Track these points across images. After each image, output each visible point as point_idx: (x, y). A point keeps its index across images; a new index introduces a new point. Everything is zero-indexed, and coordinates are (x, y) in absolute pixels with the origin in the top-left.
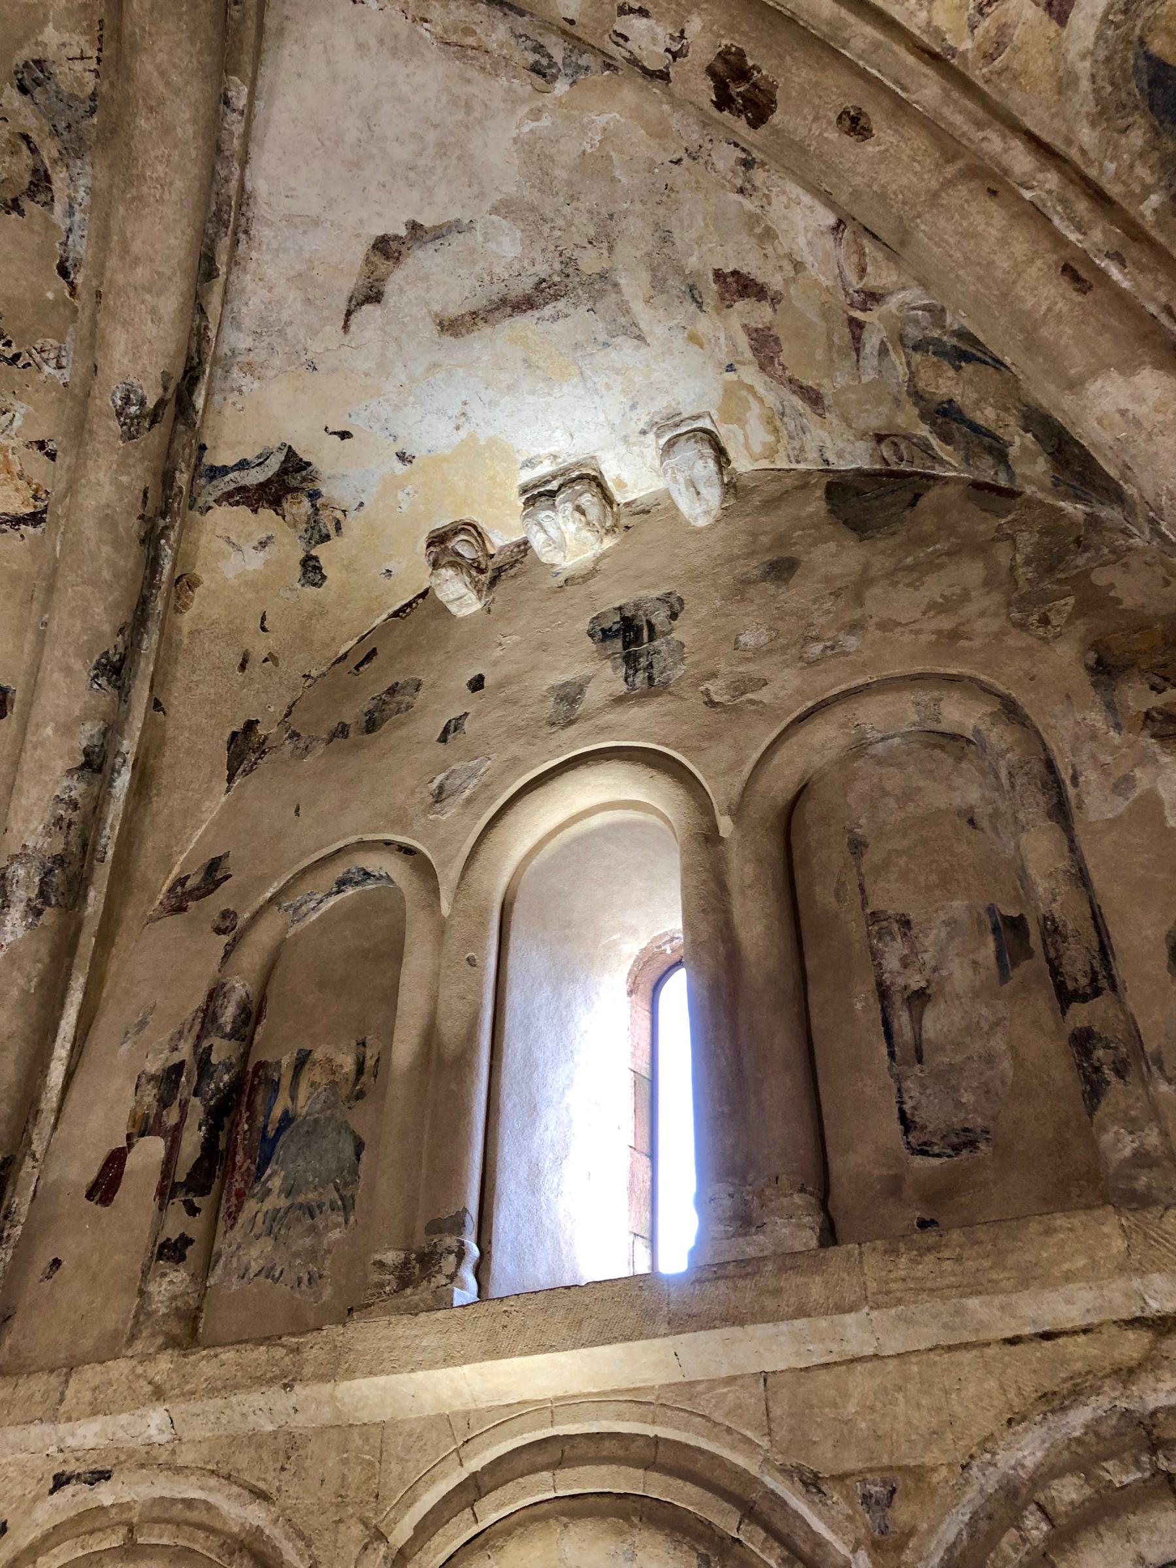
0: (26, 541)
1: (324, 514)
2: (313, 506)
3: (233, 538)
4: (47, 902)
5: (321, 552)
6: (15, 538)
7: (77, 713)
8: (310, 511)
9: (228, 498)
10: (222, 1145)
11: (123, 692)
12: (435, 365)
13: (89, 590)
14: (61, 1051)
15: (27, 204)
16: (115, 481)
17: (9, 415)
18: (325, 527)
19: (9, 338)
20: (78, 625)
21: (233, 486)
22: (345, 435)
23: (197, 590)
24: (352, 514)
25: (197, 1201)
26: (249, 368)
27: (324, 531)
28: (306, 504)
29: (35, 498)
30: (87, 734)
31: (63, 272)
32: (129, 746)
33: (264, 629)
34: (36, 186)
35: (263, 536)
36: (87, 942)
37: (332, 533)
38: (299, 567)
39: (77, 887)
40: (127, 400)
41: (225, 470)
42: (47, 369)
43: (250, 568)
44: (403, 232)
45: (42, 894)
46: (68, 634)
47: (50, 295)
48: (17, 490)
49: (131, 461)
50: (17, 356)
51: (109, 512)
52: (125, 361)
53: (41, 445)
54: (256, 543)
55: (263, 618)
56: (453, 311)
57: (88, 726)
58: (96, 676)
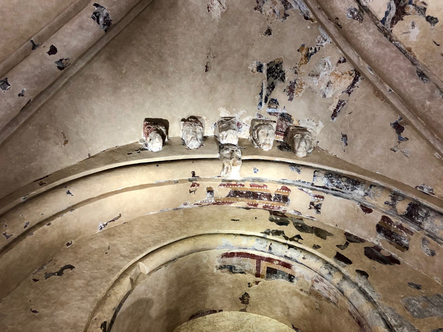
0: (359, 87)
2: (413, 5)
3: (405, 31)
5: (428, 13)
6: (356, 90)
7: (430, 91)
8: (414, 7)
13: (394, 63)
15: (288, 12)
16: (370, 34)
17: (327, 64)
18: (422, 7)
19: (310, 47)
20: (403, 73)
21: (390, 20)
23: (412, 50)
27: (423, 8)
28: (411, 6)
29: (351, 75)
31: (307, 18)
33: (438, 45)
34: (286, 5)
35: (411, 24)
37: (425, 6)
38: (428, 22)
40: (352, 13)
42: (324, 44)
43: (417, 34)
46: (402, 77)
47: (309, 27)
48: (345, 78)
49: (368, 25)
50: (315, 49)
51: (376, 41)
52: (343, 5)
53: (340, 62)
54: (411, 27)
55: (435, 43)
57: (436, 92)
58: (422, 79)
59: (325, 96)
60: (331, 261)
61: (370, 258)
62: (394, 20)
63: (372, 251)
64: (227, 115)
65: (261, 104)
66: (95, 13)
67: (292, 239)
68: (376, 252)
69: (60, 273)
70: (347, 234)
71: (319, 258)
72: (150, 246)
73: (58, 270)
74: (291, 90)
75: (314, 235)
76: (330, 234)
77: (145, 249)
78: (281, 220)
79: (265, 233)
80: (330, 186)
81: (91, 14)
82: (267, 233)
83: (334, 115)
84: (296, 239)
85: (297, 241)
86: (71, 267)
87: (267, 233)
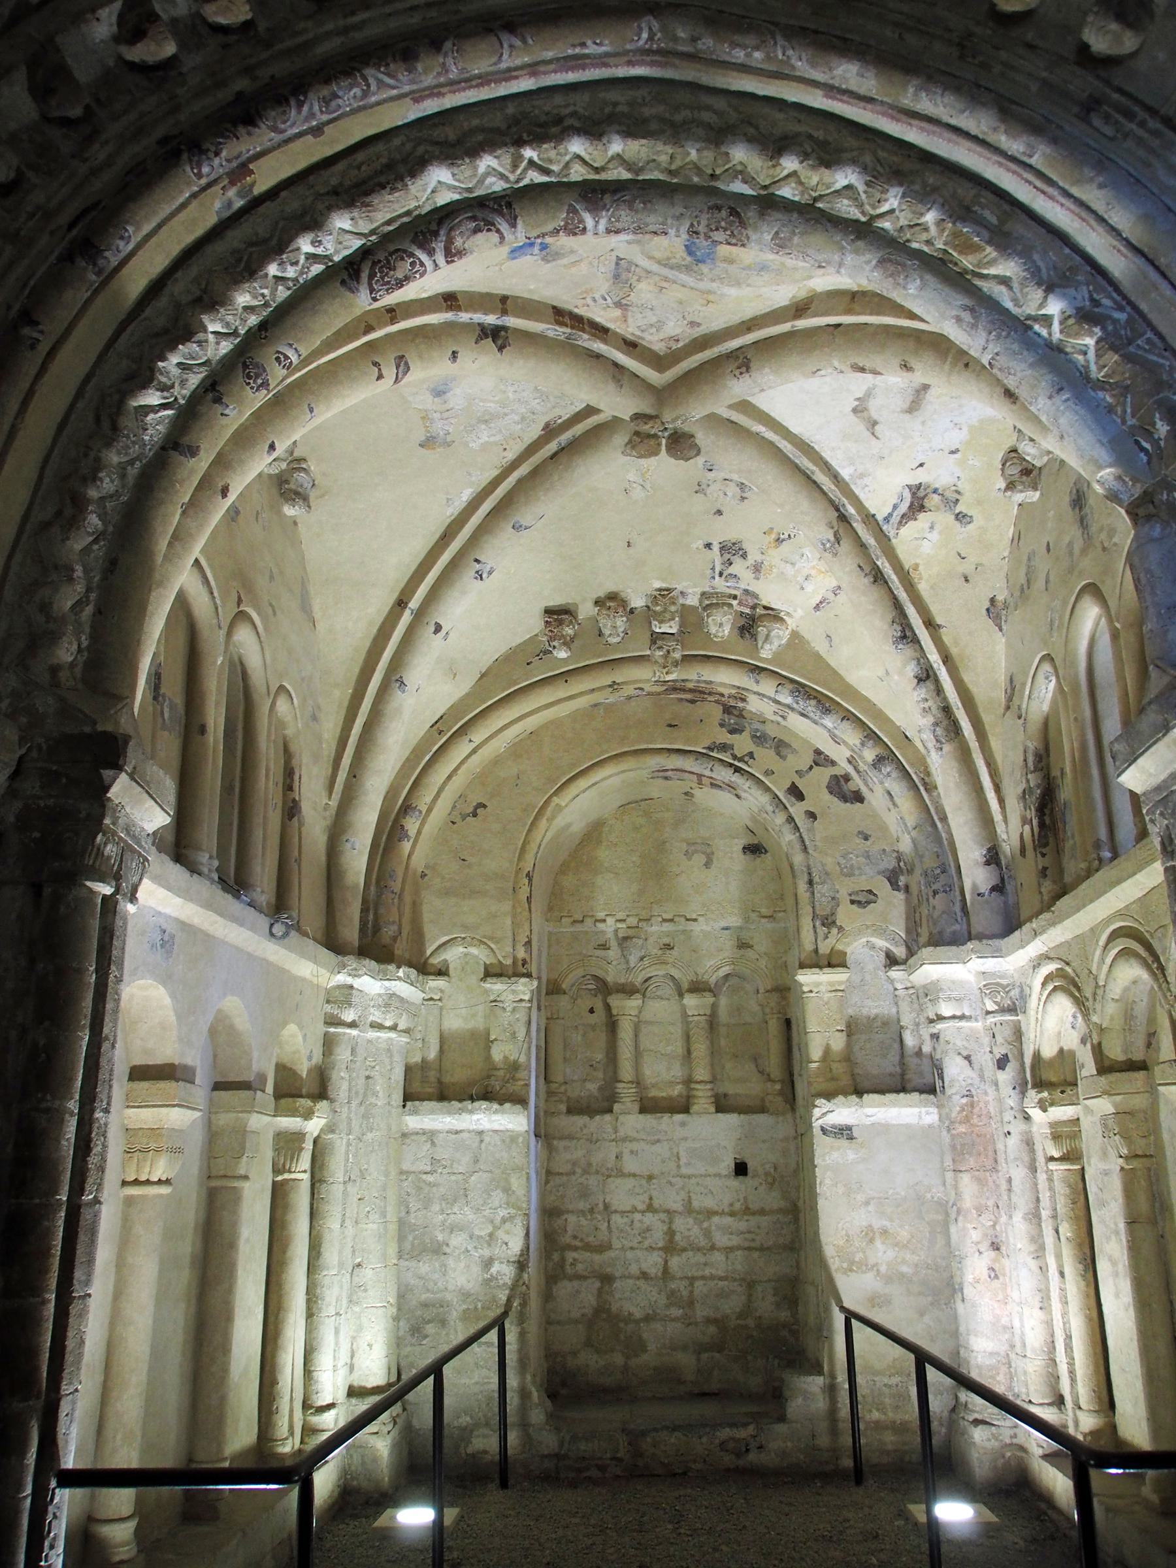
1: (948, 494)
4: (941, 743)
9: (901, 524)
10: (1048, 821)
11: (916, 641)
12: (923, 423)
14: (991, 796)
15: (745, 495)
22: (921, 465)
24: (959, 483)
25: (1044, 851)
26: (862, 476)
28: (935, 496)
30: (911, 669)
32: (934, 657)
35: (929, 525)
36: (974, 745)
37: (958, 497)
39: (954, 729)
40: (823, 544)
41: (890, 515)
44: (857, 403)
45: (937, 741)
55: (959, 555)
56: (906, 406)
59: (802, 588)
60: (781, 795)
61: (831, 793)
62: (906, 518)
63: (838, 782)
64: (664, 585)
65: (714, 578)
66: (477, 572)
67: (741, 760)
68: (842, 782)
69: (475, 815)
70: (818, 752)
71: (768, 789)
72: (564, 774)
73: (471, 810)
74: (757, 569)
75: (772, 752)
76: (794, 751)
77: (558, 778)
78: (736, 724)
79: (709, 748)
80: (795, 706)
81: (472, 574)
82: (709, 748)
83: (817, 608)
84: (746, 759)
85: (746, 763)
86: (485, 806)
87: (711, 749)
